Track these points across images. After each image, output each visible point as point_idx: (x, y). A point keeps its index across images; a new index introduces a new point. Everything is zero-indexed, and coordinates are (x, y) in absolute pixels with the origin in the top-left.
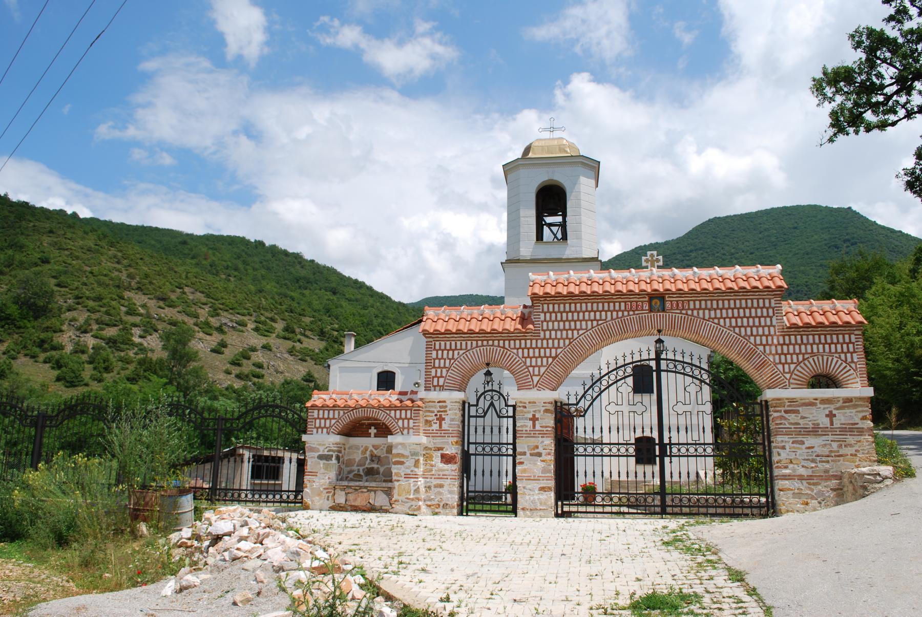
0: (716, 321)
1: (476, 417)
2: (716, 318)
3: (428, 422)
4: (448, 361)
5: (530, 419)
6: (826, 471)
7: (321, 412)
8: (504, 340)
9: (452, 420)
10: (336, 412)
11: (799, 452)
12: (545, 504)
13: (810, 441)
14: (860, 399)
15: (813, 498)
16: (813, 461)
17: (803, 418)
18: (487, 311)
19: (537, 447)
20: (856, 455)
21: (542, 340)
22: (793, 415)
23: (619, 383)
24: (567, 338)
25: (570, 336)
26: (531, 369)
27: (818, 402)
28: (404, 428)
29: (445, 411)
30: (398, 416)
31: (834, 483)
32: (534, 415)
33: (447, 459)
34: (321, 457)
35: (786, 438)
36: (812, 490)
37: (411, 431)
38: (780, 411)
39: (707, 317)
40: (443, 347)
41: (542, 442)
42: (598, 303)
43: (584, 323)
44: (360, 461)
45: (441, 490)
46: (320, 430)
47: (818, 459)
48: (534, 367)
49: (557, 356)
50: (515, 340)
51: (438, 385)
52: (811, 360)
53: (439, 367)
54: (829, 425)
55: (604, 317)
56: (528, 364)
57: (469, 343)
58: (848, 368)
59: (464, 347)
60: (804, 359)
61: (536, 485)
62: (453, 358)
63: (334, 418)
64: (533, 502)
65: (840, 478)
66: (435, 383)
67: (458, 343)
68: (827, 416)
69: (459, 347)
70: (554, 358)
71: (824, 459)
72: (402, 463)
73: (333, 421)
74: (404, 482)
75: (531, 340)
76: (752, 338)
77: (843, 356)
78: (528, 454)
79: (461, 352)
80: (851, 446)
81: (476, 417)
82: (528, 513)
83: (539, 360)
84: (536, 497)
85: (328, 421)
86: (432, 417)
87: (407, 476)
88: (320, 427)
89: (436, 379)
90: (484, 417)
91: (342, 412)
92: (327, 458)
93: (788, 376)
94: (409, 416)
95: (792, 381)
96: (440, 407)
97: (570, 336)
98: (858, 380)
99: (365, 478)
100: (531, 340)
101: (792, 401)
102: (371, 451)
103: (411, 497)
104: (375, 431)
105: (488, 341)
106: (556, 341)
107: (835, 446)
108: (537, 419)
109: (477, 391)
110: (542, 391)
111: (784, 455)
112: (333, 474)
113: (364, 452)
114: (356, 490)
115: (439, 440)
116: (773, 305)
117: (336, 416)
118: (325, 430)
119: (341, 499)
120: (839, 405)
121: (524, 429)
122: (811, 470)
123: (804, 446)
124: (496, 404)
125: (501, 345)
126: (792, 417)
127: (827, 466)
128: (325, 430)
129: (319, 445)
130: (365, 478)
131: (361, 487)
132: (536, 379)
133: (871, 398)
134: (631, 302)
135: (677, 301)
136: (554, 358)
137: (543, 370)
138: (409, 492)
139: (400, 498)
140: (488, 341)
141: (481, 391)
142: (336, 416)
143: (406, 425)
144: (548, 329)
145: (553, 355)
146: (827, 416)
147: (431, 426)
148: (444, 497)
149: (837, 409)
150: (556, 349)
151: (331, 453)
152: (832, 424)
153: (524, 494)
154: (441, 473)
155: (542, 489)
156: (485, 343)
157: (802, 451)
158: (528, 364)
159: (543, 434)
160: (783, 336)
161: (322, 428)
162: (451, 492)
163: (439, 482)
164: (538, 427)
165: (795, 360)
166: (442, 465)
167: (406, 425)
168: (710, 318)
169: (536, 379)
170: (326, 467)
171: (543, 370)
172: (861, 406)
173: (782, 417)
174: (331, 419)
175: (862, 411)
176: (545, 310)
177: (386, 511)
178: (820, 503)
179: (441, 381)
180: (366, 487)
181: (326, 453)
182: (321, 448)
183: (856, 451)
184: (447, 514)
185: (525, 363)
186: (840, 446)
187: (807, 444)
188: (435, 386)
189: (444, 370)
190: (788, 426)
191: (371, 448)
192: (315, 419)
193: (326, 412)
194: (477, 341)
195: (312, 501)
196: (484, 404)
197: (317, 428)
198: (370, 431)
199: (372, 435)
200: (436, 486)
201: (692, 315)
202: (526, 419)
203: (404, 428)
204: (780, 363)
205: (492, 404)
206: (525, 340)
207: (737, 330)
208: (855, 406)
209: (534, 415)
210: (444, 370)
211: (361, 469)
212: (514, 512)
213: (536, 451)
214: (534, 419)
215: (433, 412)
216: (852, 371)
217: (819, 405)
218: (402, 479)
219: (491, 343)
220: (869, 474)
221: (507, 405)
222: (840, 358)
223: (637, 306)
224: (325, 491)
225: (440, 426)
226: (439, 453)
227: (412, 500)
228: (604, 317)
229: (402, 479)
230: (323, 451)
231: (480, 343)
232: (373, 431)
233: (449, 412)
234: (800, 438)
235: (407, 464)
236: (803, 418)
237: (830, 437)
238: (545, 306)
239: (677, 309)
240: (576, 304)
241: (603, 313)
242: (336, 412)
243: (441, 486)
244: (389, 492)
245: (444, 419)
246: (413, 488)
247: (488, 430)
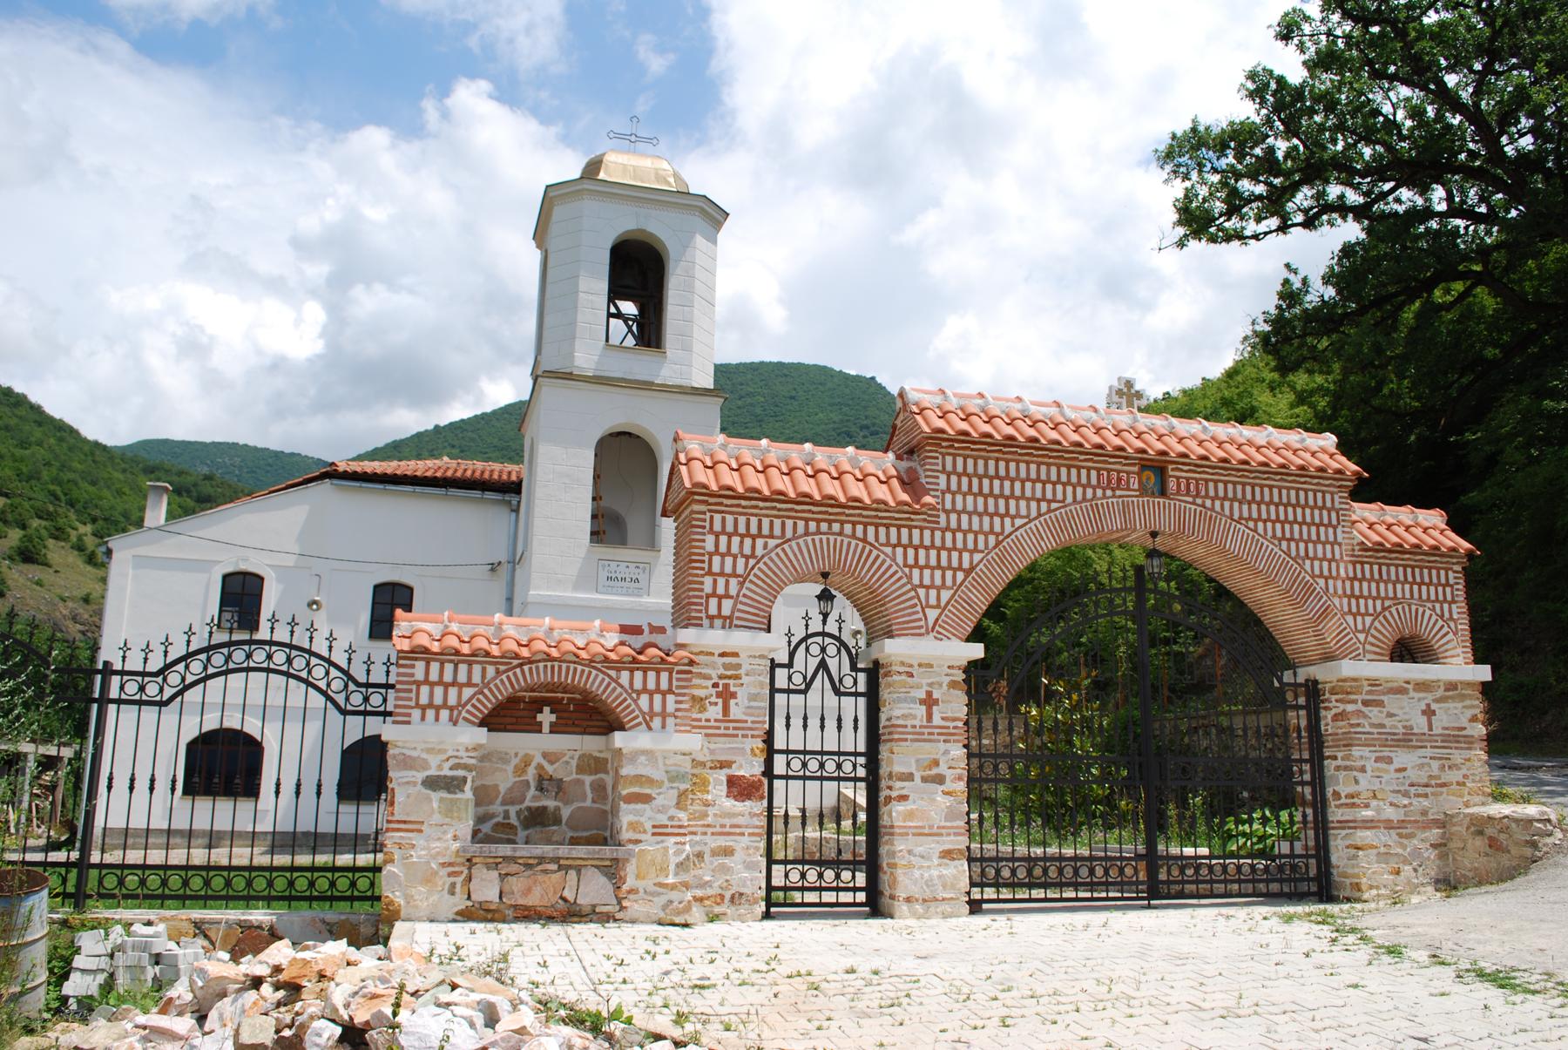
0: (1251, 524)
1: (788, 691)
2: (1250, 518)
3: (699, 702)
4: (741, 562)
5: (922, 702)
6: (1424, 813)
7: (435, 666)
8: (865, 525)
9: (753, 697)
10: (477, 669)
11: (1386, 777)
12: (953, 887)
13: (1402, 758)
14: (1469, 684)
15: (1406, 862)
16: (1406, 794)
17: (1390, 715)
18: (819, 457)
19: (936, 763)
20: (1464, 784)
21: (943, 531)
22: (1376, 710)
24: (992, 532)
26: (922, 592)
28: (652, 714)
29: (737, 677)
30: (638, 685)
31: (1435, 834)
32: (929, 694)
34: (432, 783)
35: (1365, 751)
36: (1404, 847)
37: (670, 721)
38: (1354, 702)
39: (1236, 516)
40: (730, 528)
41: (946, 752)
42: (1049, 465)
43: (1023, 503)
44: (511, 789)
45: (727, 861)
46: (430, 713)
47: (1412, 789)
48: (927, 588)
49: (972, 568)
50: (887, 527)
51: (719, 616)
52: (1393, 610)
53: (722, 574)
54: (1426, 730)
55: (1060, 496)
56: (916, 581)
57: (789, 523)
58: (1446, 629)
59: (777, 531)
60: (1384, 609)
61: (934, 847)
62: (753, 555)
63: (469, 684)
64: (929, 883)
65: (1441, 824)
66: (713, 610)
67: (766, 522)
68: (1424, 713)
69: (766, 531)
70: (968, 572)
71: (1421, 790)
72: (646, 799)
73: (468, 692)
74: (650, 846)
75: (922, 529)
76: (1308, 562)
77: (1438, 606)
78: (918, 779)
79: (772, 543)
81: (788, 691)
82: (919, 908)
83: (938, 573)
84: (935, 873)
85: (453, 692)
86: (703, 690)
87: (660, 831)
88: (430, 705)
89: (713, 602)
90: (804, 692)
91: (491, 671)
92: (450, 784)
93: (1362, 637)
94: (664, 685)
95: (1368, 647)
96: (726, 667)
97: (997, 528)
98: (1459, 650)
99: (522, 834)
100: (922, 529)
101: (1374, 683)
102: (540, 767)
103: (671, 880)
104: (553, 718)
105: (830, 522)
106: (970, 537)
108: (936, 702)
109: (789, 634)
110: (946, 642)
111: (1365, 783)
112: (466, 827)
113: (521, 769)
114: (528, 866)
116: (1337, 506)
117: (477, 678)
118: (444, 714)
119: (487, 889)
120: (1440, 693)
121: (909, 723)
122: (1402, 811)
123: (1392, 768)
124: (832, 664)
125: (859, 533)
126: (1373, 712)
127: (1425, 803)
128: (444, 714)
129: (429, 751)
130: (522, 834)
131: (542, 860)
132: (932, 614)
133: (1484, 684)
134: (1109, 471)
135: (1187, 479)
136: (968, 572)
138: (664, 870)
139: (640, 884)
140: (830, 522)
141: (799, 633)
142: (477, 678)
143: (657, 707)
144: (954, 510)
145: (966, 565)
146: (1424, 713)
147: (703, 709)
148: (734, 879)
149: (1437, 701)
150: (971, 552)
151: (460, 773)
152: (1431, 729)
153: (910, 866)
154: (727, 822)
155: (947, 854)
156: (836, 527)
157: (1390, 775)
158: (916, 581)
159: (947, 736)
160: (1354, 563)
161: (438, 709)
162: (749, 866)
163: (722, 842)
164: (937, 720)
166: (730, 804)
167: (657, 707)
168: (1241, 518)
169: (932, 614)
170: (449, 810)
172: (1470, 697)
173: (1359, 713)
174: (461, 686)
176: (949, 467)
177: (606, 918)
178: (1415, 870)
179: (727, 606)
180: (556, 860)
181: (446, 772)
182: (434, 761)
183: (1465, 776)
184: (742, 919)
185: (910, 577)
187: (1396, 765)
188: (711, 618)
189: (733, 582)
190: (1368, 729)
191: (538, 759)
192: (418, 684)
193: (449, 667)
194: (807, 520)
195: (409, 898)
196: (805, 662)
197: (424, 709)
198: (540, 717)
199: (546, 728)
200: (715, 853)
201: (1213, 509)
202: (913, 700)
203: (652, 714)
205: (823, 665)
206: (910, 528)
207: (1284, 544)
208: (1463, 697)
209: (929, 694)
210: (733, 582)
211: (513, 810)
212: (876, 905)
213: (935, 771)
214: (929, 702)
215: (708, 677)
216: (1451, 636)
217: (1412, 694)
218: (647, 837)
219: (824, 527)
220: (1539, 821)
221: (854, 667)
222: (1434, 609)
223: (1119, 480)
224: (444, 872)
225: (930, 717)
226: (722, 775)
227: (673, 887)
228: (1060, 496)
229: (647, 837)
230: (437, 766)
231: (813, 525)
232: (546, 717)
233: (745, 680)
234: (1386, 752)
235: (660, 801)
236: (1390, 715)
237: (1429, 752)
238: (949, 459)
239: (1188, 494)
240: (1007, 462)
241: (1059, 488)
242: (477, 669)
244: (613, 870)
245: (734, 695)
246: (674, 860)
247: (814, 723)
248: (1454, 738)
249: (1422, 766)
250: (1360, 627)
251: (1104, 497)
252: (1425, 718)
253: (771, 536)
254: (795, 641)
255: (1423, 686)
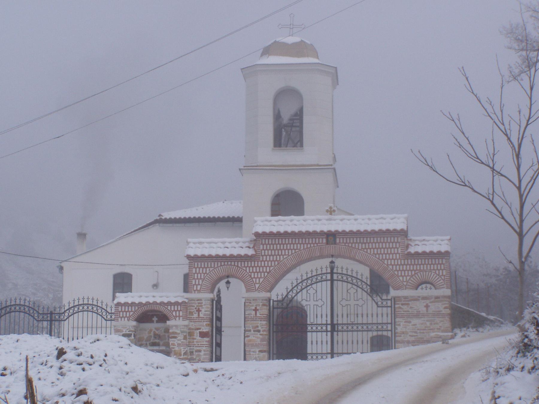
2: (365, 248)
4: (203, 275)
5: (254, 310)
9: (206, 311)
13: (415, 321)
16: (416, 332)
17: (411, 308)
19: (258, 327)
22: (406, 306)
23: (308, 288)
25: (278, 259)
27: (420, 299)
28: (176, 316)
29: (201, 306)
30: (173, 309)
33: (203, 335)
39: (360, 248)
43: (287, 251)
46: (123, 319)
47: (418, 331)
51: (197, 290)
52: (419, 274)
55: (299, 248)
59: (213, 266)
60: (415, 273)
62: (206, 273)
63: (132, 311)
66: (195, 289)
68: (425, 306)
69: (209, 266)
71: (422, 331)
72: (175, 337)
73: (131, 313)
77: (437, 272)
78: (252, 331)
79: (211, 269)
80: (437, 324)
84: (257, 356)
85: (128, 314)
91: (137, 308)
94: (179, 309)
96: (199, 303)
97: (278, 259)
101: (406, 298)
102: (154, 332)
103: (182, 357)
107: (428, 324)
108: (258, 310)
113: (150, 332)
115: (197, 324)
117: (133, 310)
120: (432, 300)
123: (410, 324)
125: (236, 264)
126: (405, 307)
128: (126, 319)
132: (257, 286)
136: (268, 273)
137: (261, 280)
142: (133, 310)
143: (178, 315)
145: (268, 271)
146: (425, 306)
147: (193, 315)
149: (431, 302)
152: (427, 310)
155: (261, 351)
156: (226, 263)
158: (253, 276)
161: (124, 318)
163: (198, 348)
164: (258, 315)
165: (410, 274)
167: (178, 315)
169: (257, 286)
171: (261, 280)
175: (445, 304)
185: (251, 276)
186: (431, 324)
187: (412, 323)
188: (195, 291)
189: (201, 281)
191: (154, 330)
192: (120, 312)
193: (127, 307)
194: (221, 262)
197: (121, 318)
198: (153, 319)
199: (155, 322)
200: (197, 351)
202: (251, 310)
204: (401, 276)
207: (377, 256)
209: (256, 308)
213: (257, 329)
215: (194, 306)
232: (155, 319)
233: (204, 307)
235: (179, 338)
242: (133, 307)
243: (200, 351)
245: (201, 311)
248: (437, 314)
249: (422, 324)
250: (405, 280)
251: (314, 246)
252: (425, 309)
253: (211, 267)
254: (289, 290)
255: (424, 298)
